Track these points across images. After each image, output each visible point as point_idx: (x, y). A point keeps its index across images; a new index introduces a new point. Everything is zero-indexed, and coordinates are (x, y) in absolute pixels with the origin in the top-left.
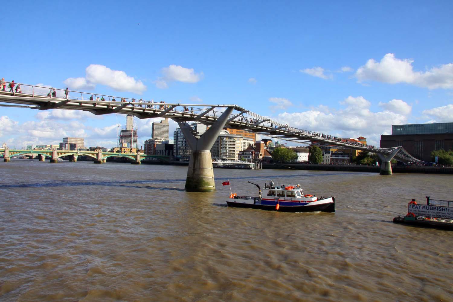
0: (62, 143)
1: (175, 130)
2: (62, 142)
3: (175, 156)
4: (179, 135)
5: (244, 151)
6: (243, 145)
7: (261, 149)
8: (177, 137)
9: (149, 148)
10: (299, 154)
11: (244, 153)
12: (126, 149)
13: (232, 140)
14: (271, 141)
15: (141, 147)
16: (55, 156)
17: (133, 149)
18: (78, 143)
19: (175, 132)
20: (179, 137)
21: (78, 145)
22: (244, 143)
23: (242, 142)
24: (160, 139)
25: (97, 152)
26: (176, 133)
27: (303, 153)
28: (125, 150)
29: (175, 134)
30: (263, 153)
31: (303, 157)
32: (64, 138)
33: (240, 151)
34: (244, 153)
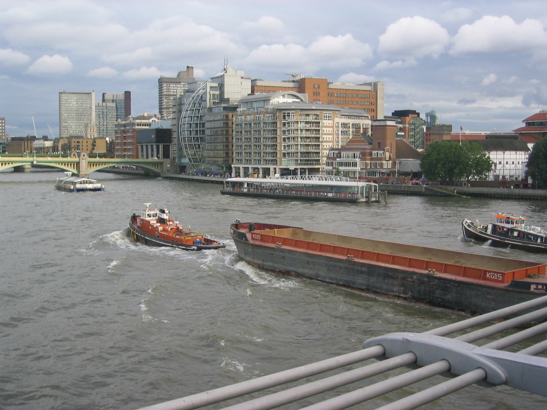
5: (343, 148)
6: (340, 129)
7: (388, 142)
8: (180, 111)
9: (125, 138)
10: (495, 156)
11: (343, 153)
12: (80, 140)
13: (311, 119)
14: (416, 116)
17: (97, 141)
22: (344, 125)
23: (338, 123)
24: (149, 118)
27: (507, 153)
28: (78, 142)
30: (394, 150)
31: (507, 163)
33: (332, 149)
34: (343, 153)
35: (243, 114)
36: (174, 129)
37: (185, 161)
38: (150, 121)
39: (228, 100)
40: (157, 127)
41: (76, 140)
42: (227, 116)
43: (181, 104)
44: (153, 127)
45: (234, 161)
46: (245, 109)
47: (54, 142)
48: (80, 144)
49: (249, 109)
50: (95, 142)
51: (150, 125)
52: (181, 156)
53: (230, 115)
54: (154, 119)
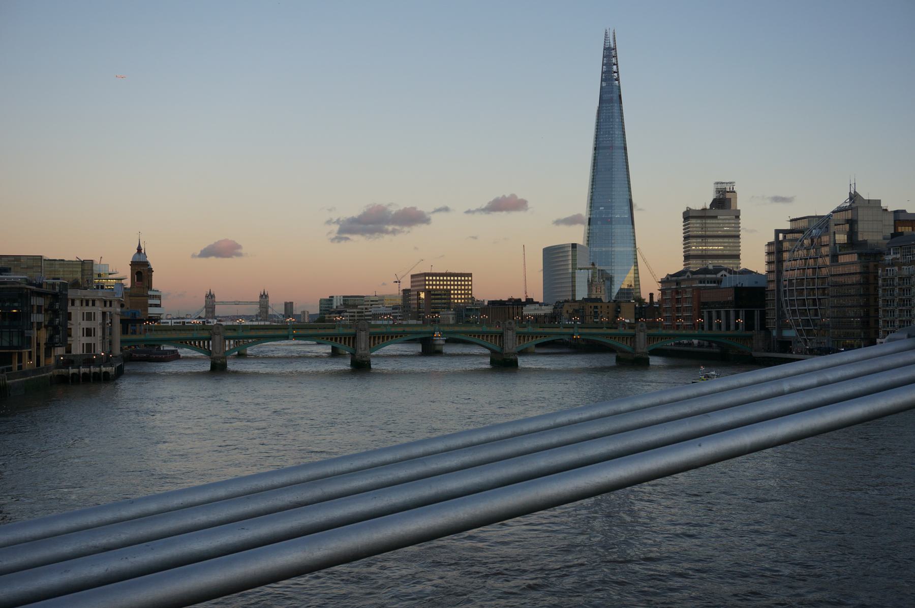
0: (409, 290)
1: (772, 239)
2: (408, 286)
3: (774, 333)
4: (786, 255)
8: (780, 261)
12: (599, 305)
15: (651, 295)
16: (363, 346)
18: (454, 290)
19: (769, 244)
20: (786, 265)
21: (454, 294)
25: (501, 330)
26: (773, 248)
28: (596, 307)
29: (769, 253)
32: (412, 276)
35: (893, 264)
36: (772, 286)
37: (789, 333)
38: (719, 275)
39: (865, 243)
40: (733, 284)
41: (593, 305)
42: (867, 267)
43: (780, 251)
44: (726, 284)
45: (881, 333)
46: (898, 256)
47: (555, 308)
48: (599, 310)
49: (904, 256)
50: (619, 307)
51: (719, 281)
52: (783, 326)
53: (871, 265)
54: (723, 272)
